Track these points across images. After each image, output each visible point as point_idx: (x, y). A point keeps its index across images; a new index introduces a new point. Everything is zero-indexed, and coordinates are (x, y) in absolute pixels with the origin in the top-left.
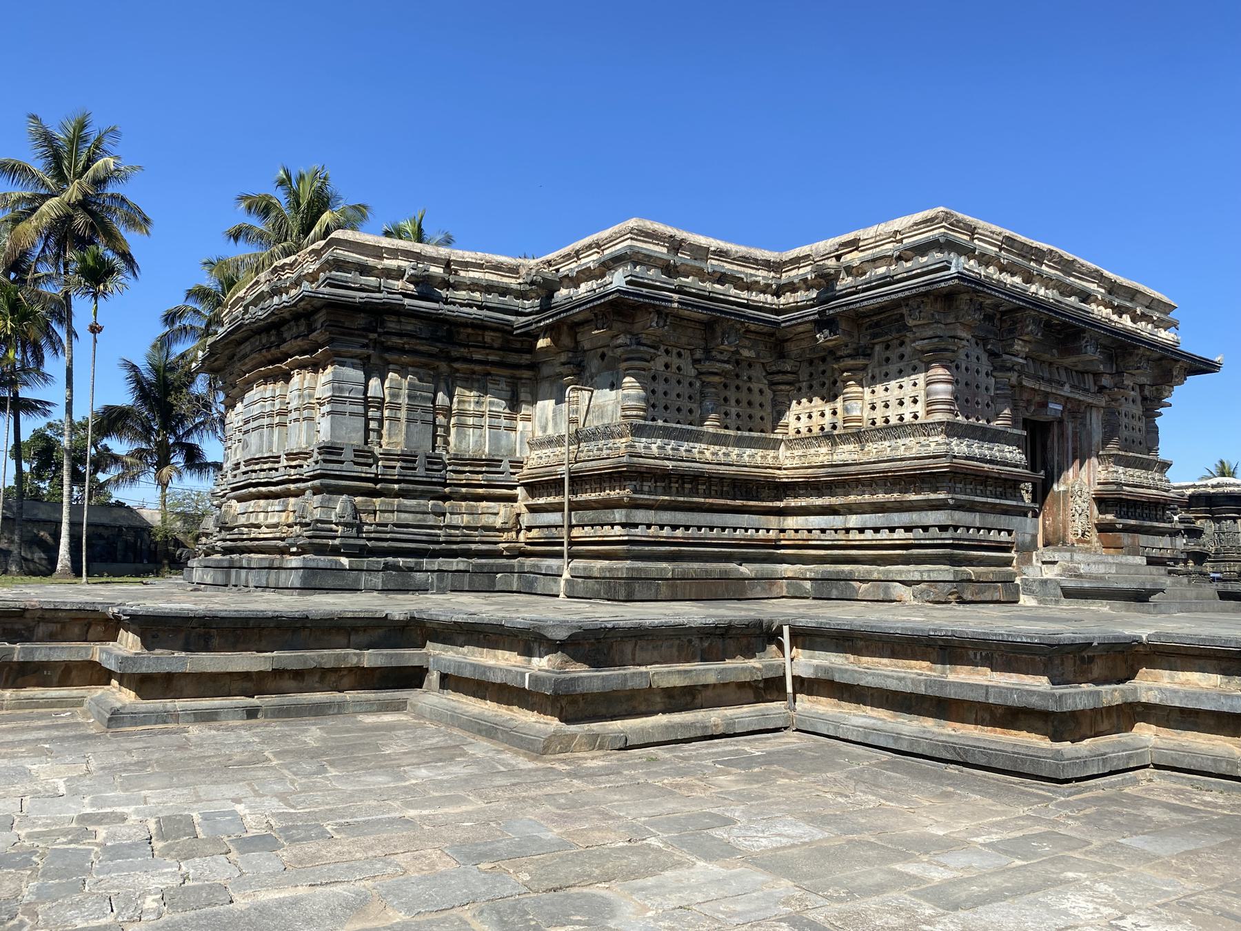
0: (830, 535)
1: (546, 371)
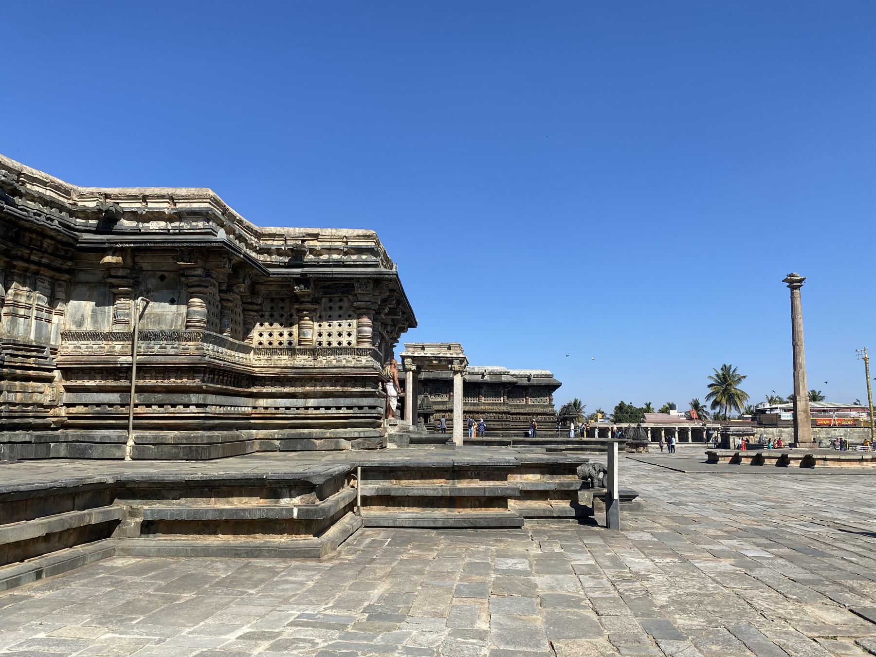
1: (83, 277)
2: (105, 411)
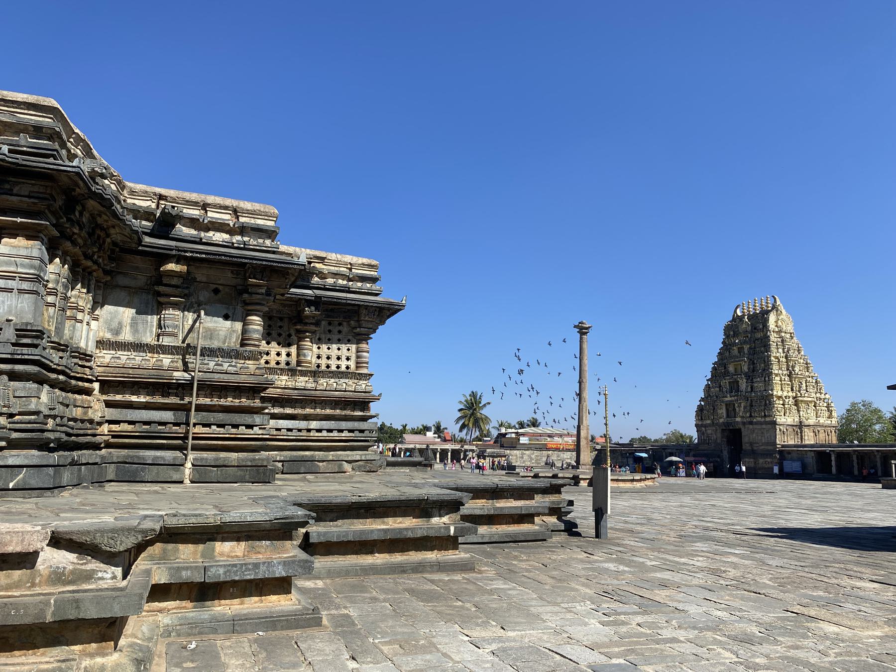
0: (295, 433)
1: (121, 280)
2: (156, 430)
